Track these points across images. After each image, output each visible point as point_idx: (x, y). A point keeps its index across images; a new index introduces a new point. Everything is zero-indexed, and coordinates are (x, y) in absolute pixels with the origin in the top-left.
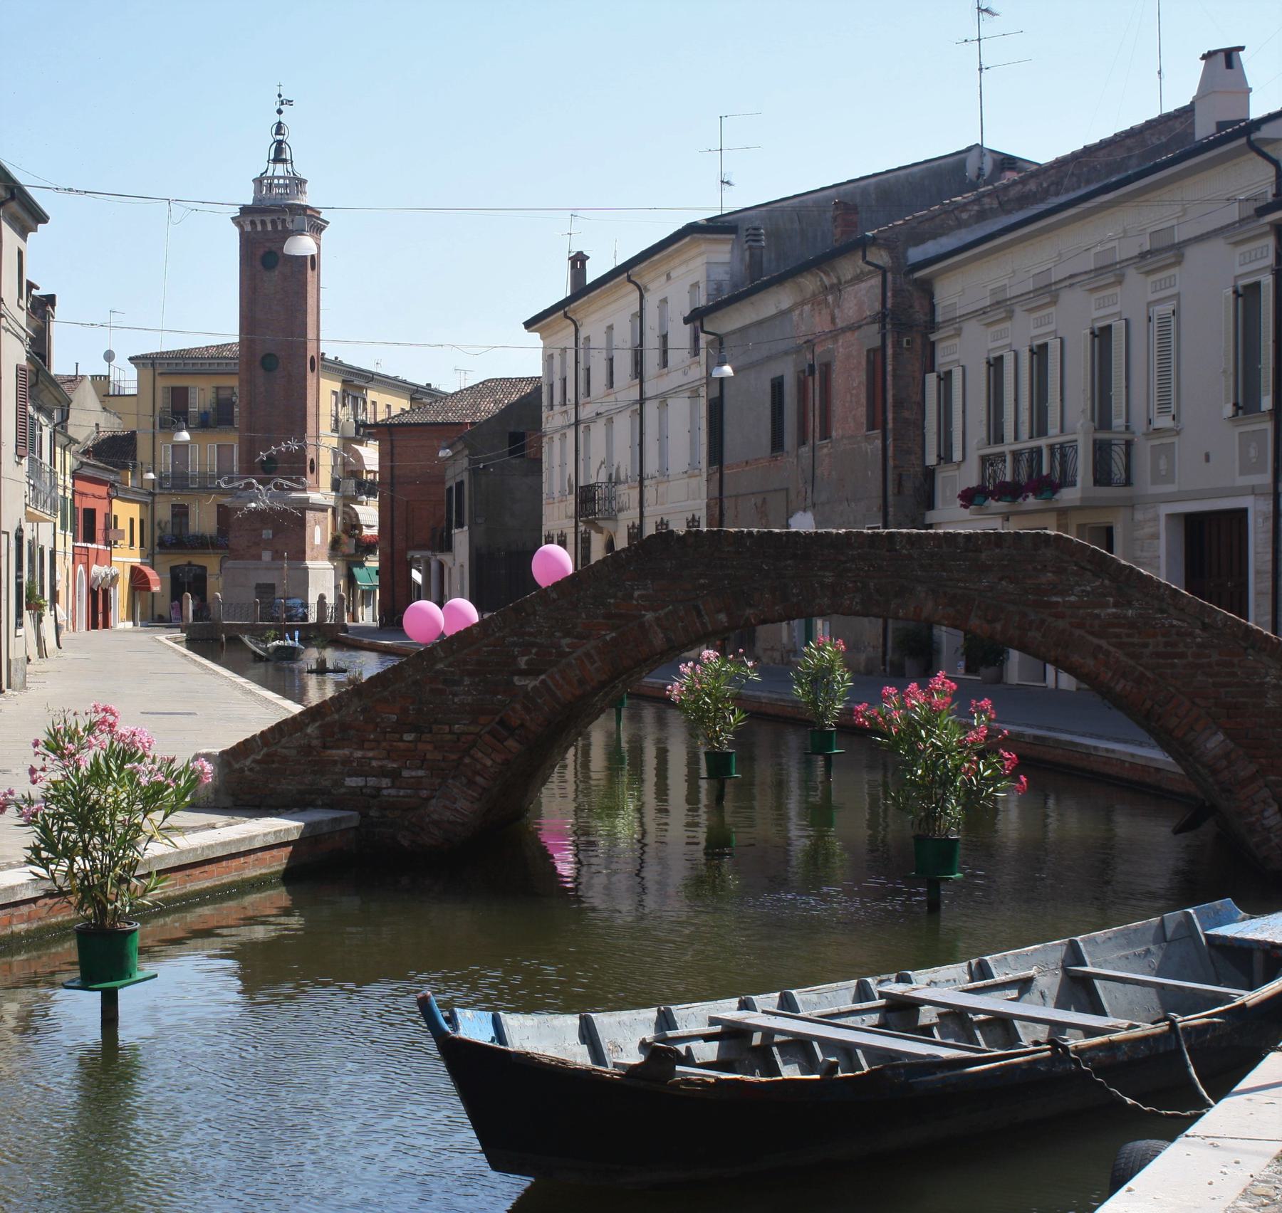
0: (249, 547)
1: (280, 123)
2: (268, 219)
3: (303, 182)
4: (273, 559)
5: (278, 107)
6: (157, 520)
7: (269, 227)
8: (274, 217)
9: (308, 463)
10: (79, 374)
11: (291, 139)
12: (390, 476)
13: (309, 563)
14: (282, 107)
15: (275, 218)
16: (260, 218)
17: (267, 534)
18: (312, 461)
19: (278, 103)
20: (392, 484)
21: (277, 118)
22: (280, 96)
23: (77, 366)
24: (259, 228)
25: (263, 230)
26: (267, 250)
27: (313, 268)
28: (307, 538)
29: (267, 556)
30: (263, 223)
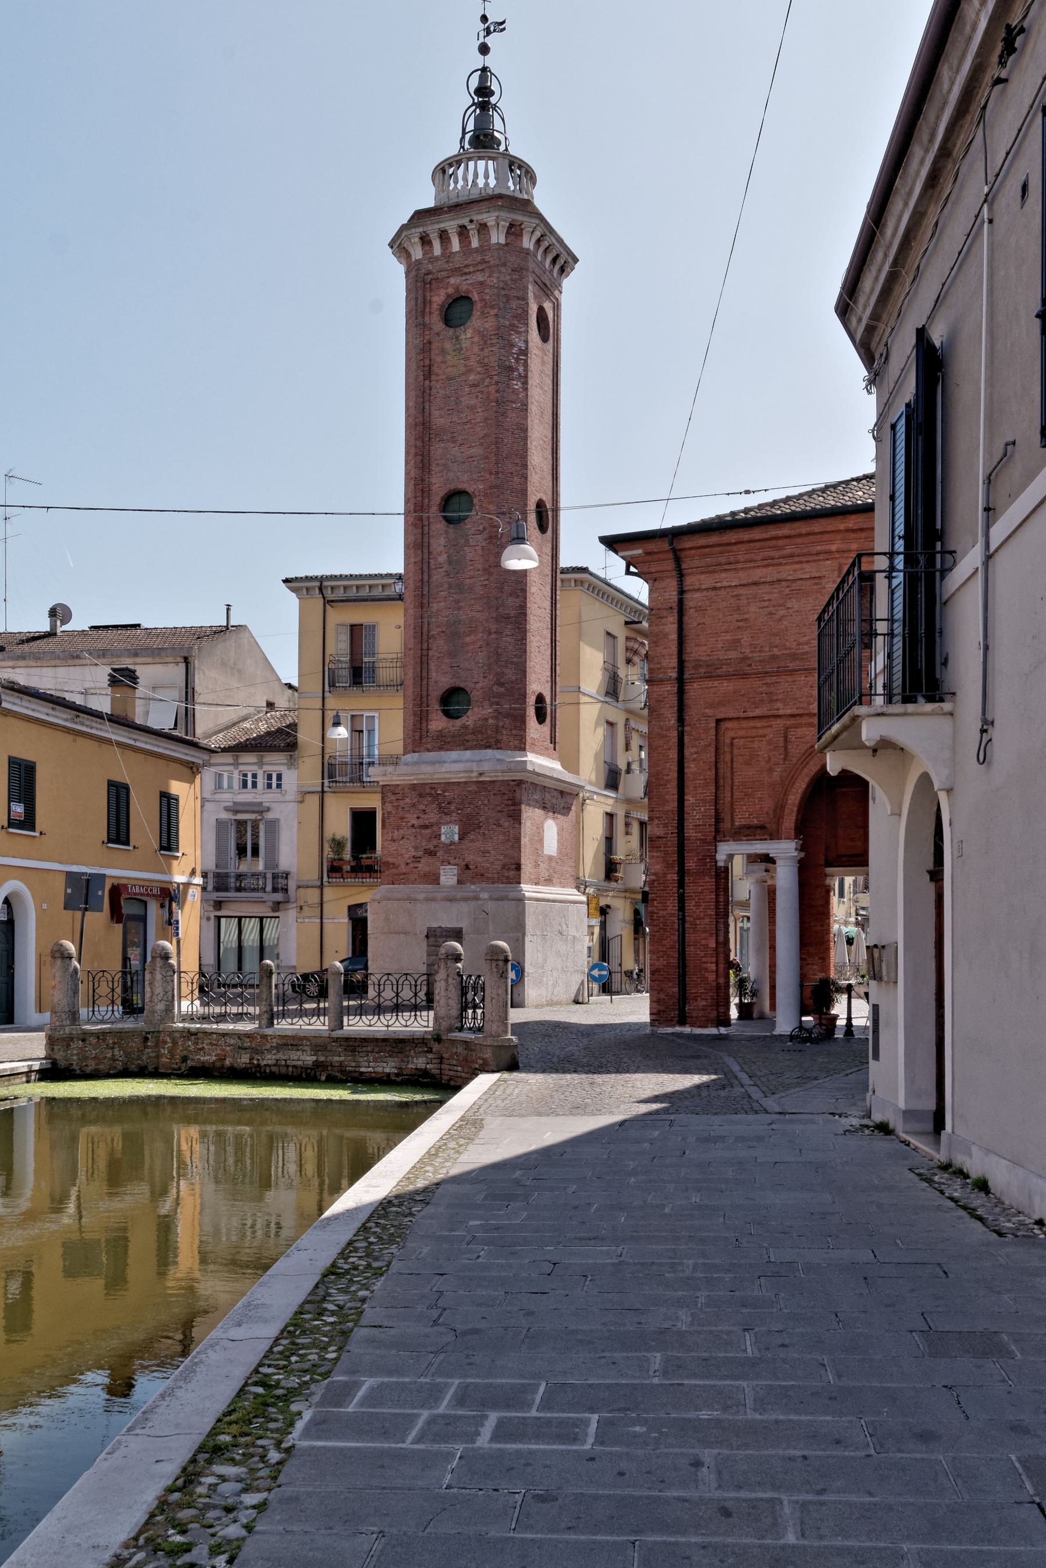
0: (416, 859)
1: (484, 70)
2: (451, 225)
3: (524, 172)
4: (459, 882)
5: (481, 40)
6: (328, 835)
7: (456, 245)
8: (461, 222)
9: (531, 700)
10: (232, 623)
11: (504, 100)
12: (674, 662)
13: (528, 889)
14: (490, 41)
15: (465, 221)
16: (437, 226)
17: (450, 832)
18: (540, 699)
19: (482, 34)
20: (681, 681)
21: (479, 61)
22: (484, 18)
23: (228, 610)
24: (437, 249)
25: (443, 254)
26: (450, 290)
27: (545, 339)
28: (525, 841)
29: (448, 876)
30: (444, 236)
